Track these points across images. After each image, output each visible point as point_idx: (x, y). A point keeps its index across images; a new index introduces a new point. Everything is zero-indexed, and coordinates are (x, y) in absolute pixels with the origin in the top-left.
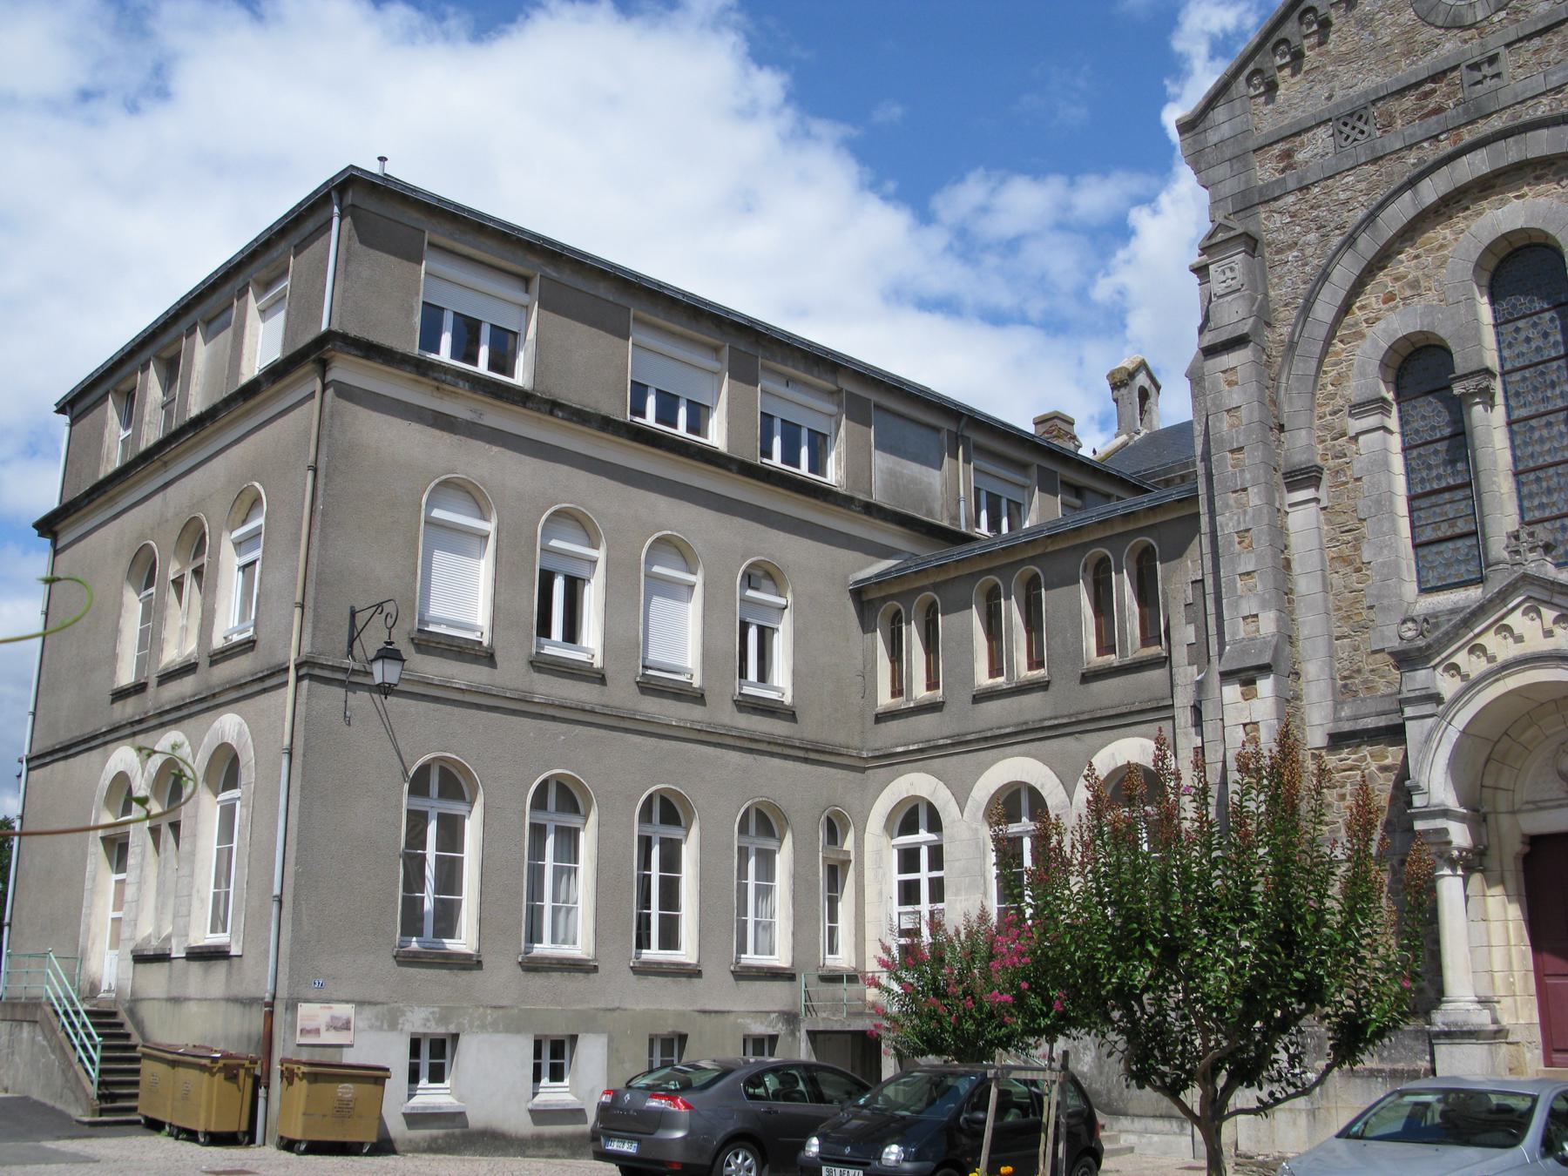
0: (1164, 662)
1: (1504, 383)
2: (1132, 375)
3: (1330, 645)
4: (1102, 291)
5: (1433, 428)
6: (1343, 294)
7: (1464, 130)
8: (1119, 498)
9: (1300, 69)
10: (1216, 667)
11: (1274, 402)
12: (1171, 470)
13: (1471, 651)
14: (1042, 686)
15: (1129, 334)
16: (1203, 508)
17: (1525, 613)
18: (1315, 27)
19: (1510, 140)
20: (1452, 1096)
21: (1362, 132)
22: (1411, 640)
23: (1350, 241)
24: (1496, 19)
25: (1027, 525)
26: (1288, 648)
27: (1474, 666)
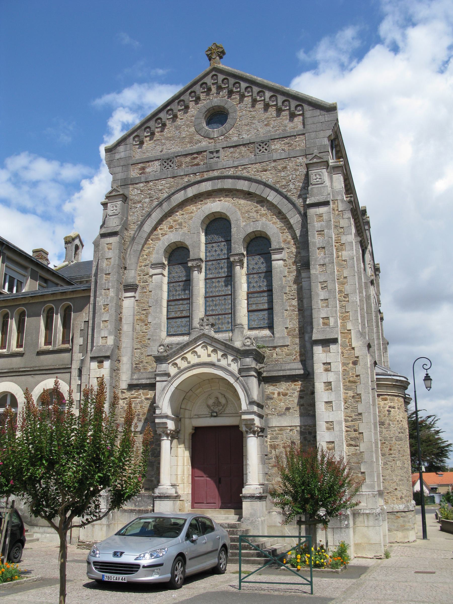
0: (69, 350)
1: (206, 264)
2: (73, 239)
3: (133, 351)
4: (67, 207)
5: (179, 277)
6: (155, 223)
7: (205, 173)
8: (61, 286)
9: (153, 139)
10: (89, 355)
11: (124, 258)
12: (83, 278)
13: (182, 359)
14: (21, 355)
15: (75, 225)
16: (92, 294)
17: (202, 347)
18: (160, 125)
19: (219, 180)
20: (158, 519)
21: (171, 166)
22: (161, 353)
23: (160, 204)
24: (220, 138)
25: (24, 291)
26: (117, 351)
27: (182, 364)
